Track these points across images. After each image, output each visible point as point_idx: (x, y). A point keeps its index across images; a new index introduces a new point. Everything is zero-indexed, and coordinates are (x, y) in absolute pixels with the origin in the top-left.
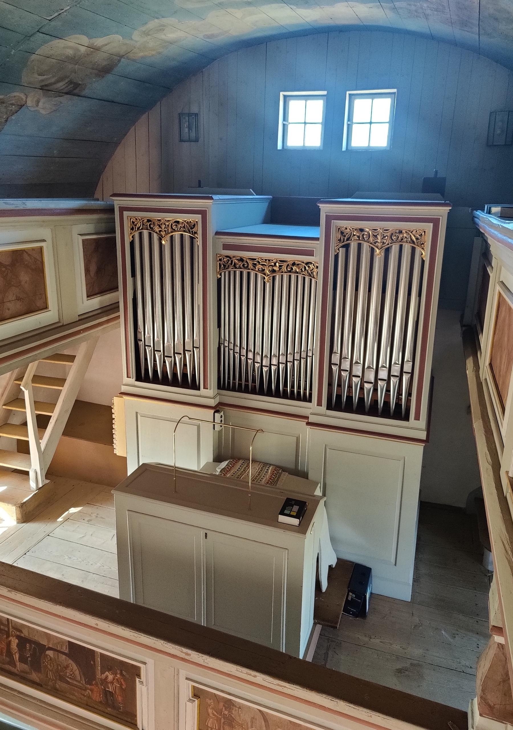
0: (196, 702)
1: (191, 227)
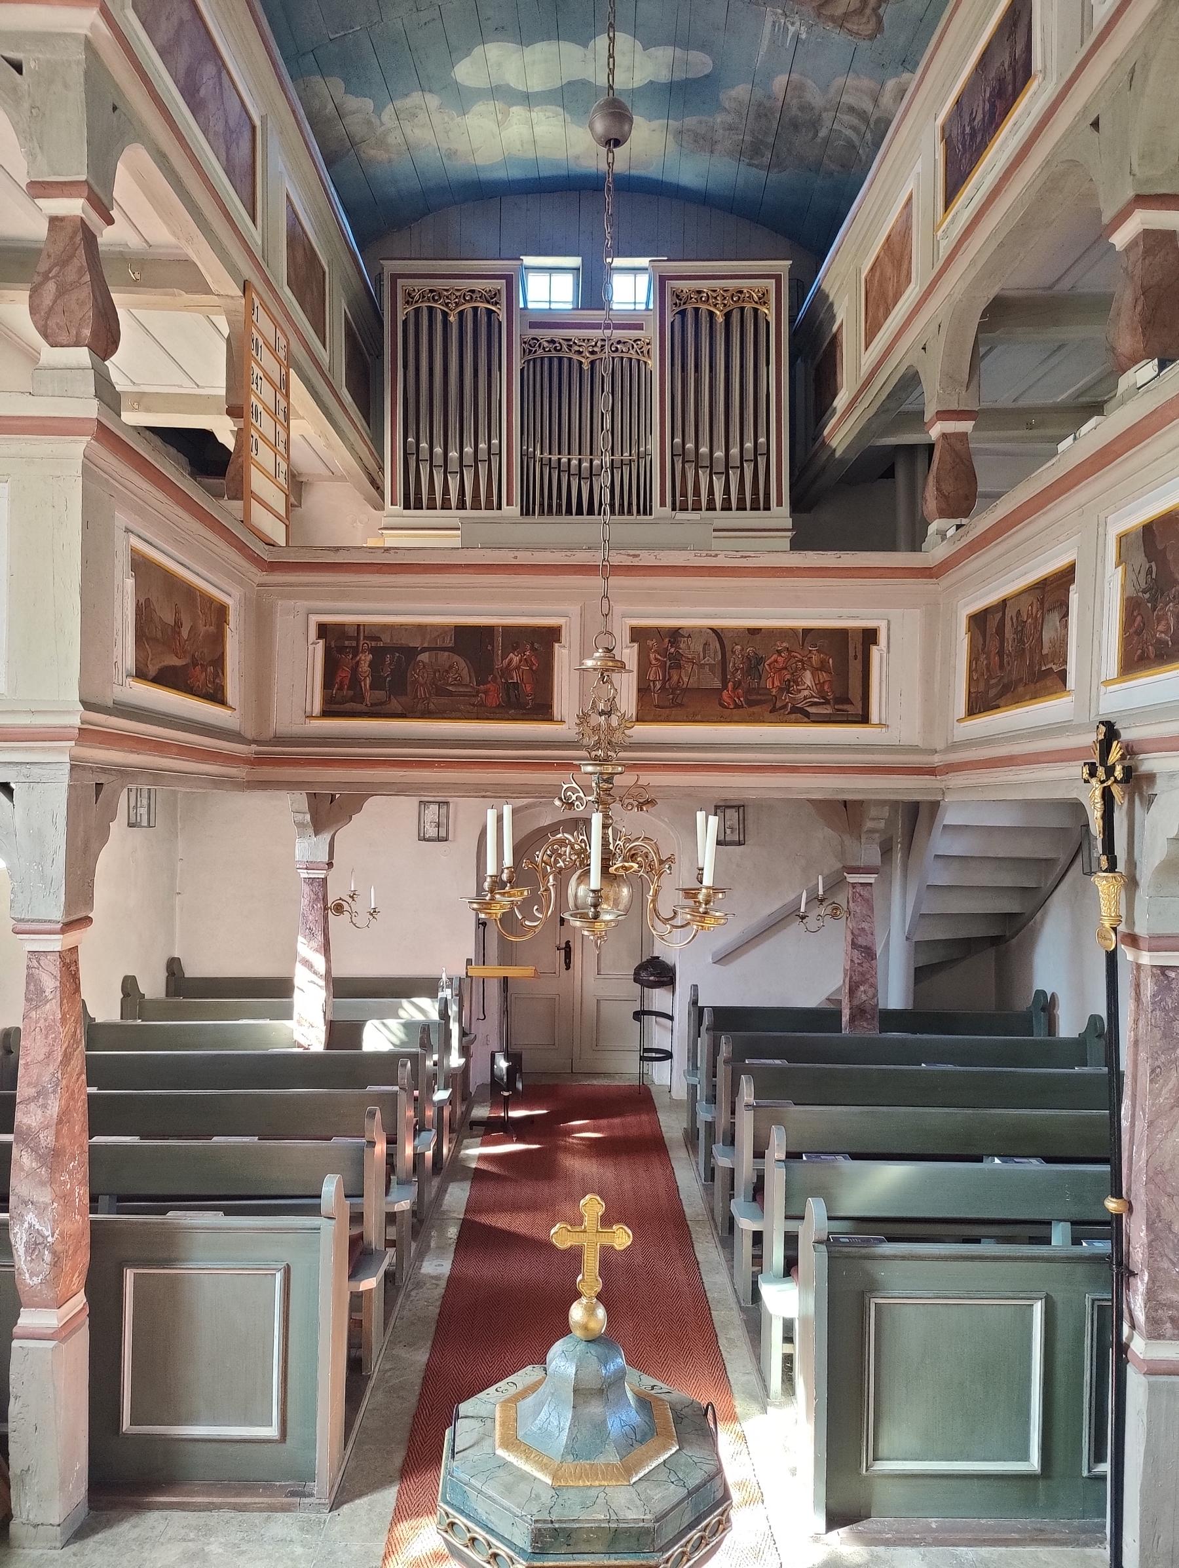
0: (636, 645)
1: (493, 297)
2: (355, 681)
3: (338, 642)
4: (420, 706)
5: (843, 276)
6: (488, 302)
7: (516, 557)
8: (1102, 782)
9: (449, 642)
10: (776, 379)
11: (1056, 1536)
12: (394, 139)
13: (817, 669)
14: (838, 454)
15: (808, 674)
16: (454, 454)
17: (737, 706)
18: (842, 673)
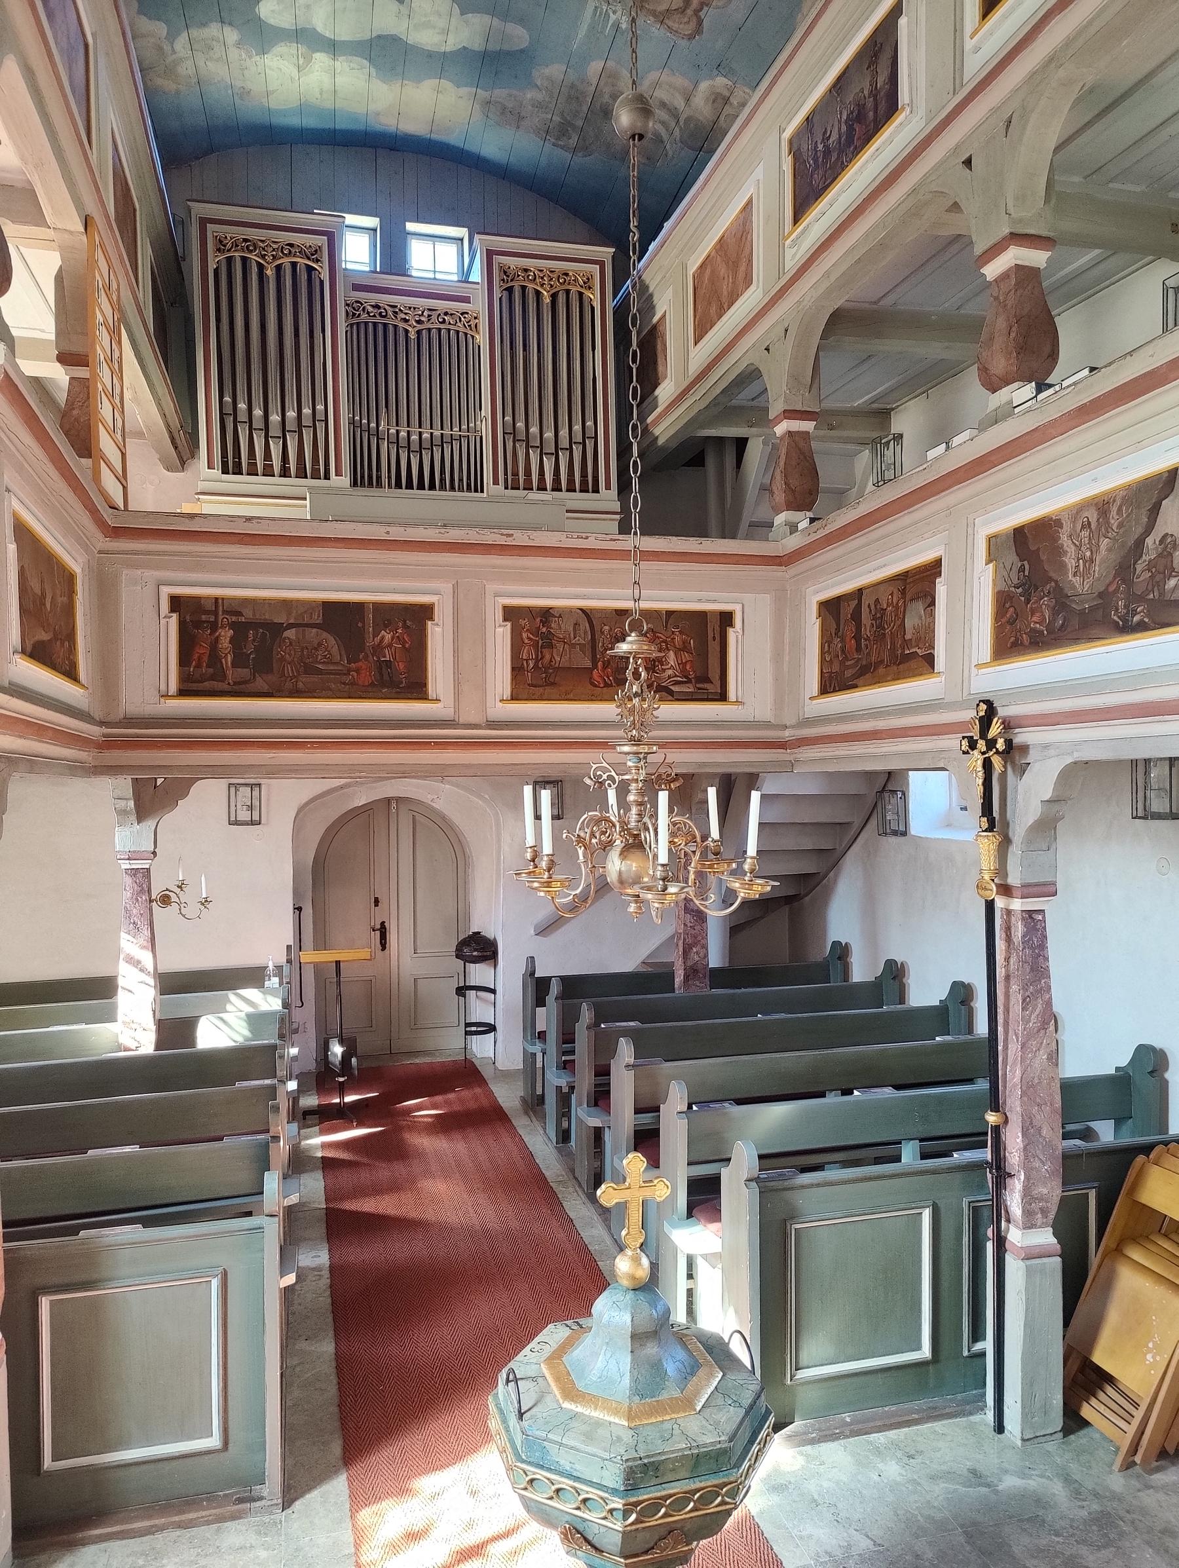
0: (509, 624)
1: (313, 254)
2: (214, 657)
3: (195, 618)
4: (289, 685)
5: (670, 269)
6: (309, 259)
7: (388, 533)
8: (983, 753)
9: (317, 618)
10: (601, 363)
11: (947, 1410)
12: (186, 69)
13: (680, 650)
14: (660, 442)
15: (672, 654)
16: (275, 418)
17: (607, 685)
18: (702, 654)
